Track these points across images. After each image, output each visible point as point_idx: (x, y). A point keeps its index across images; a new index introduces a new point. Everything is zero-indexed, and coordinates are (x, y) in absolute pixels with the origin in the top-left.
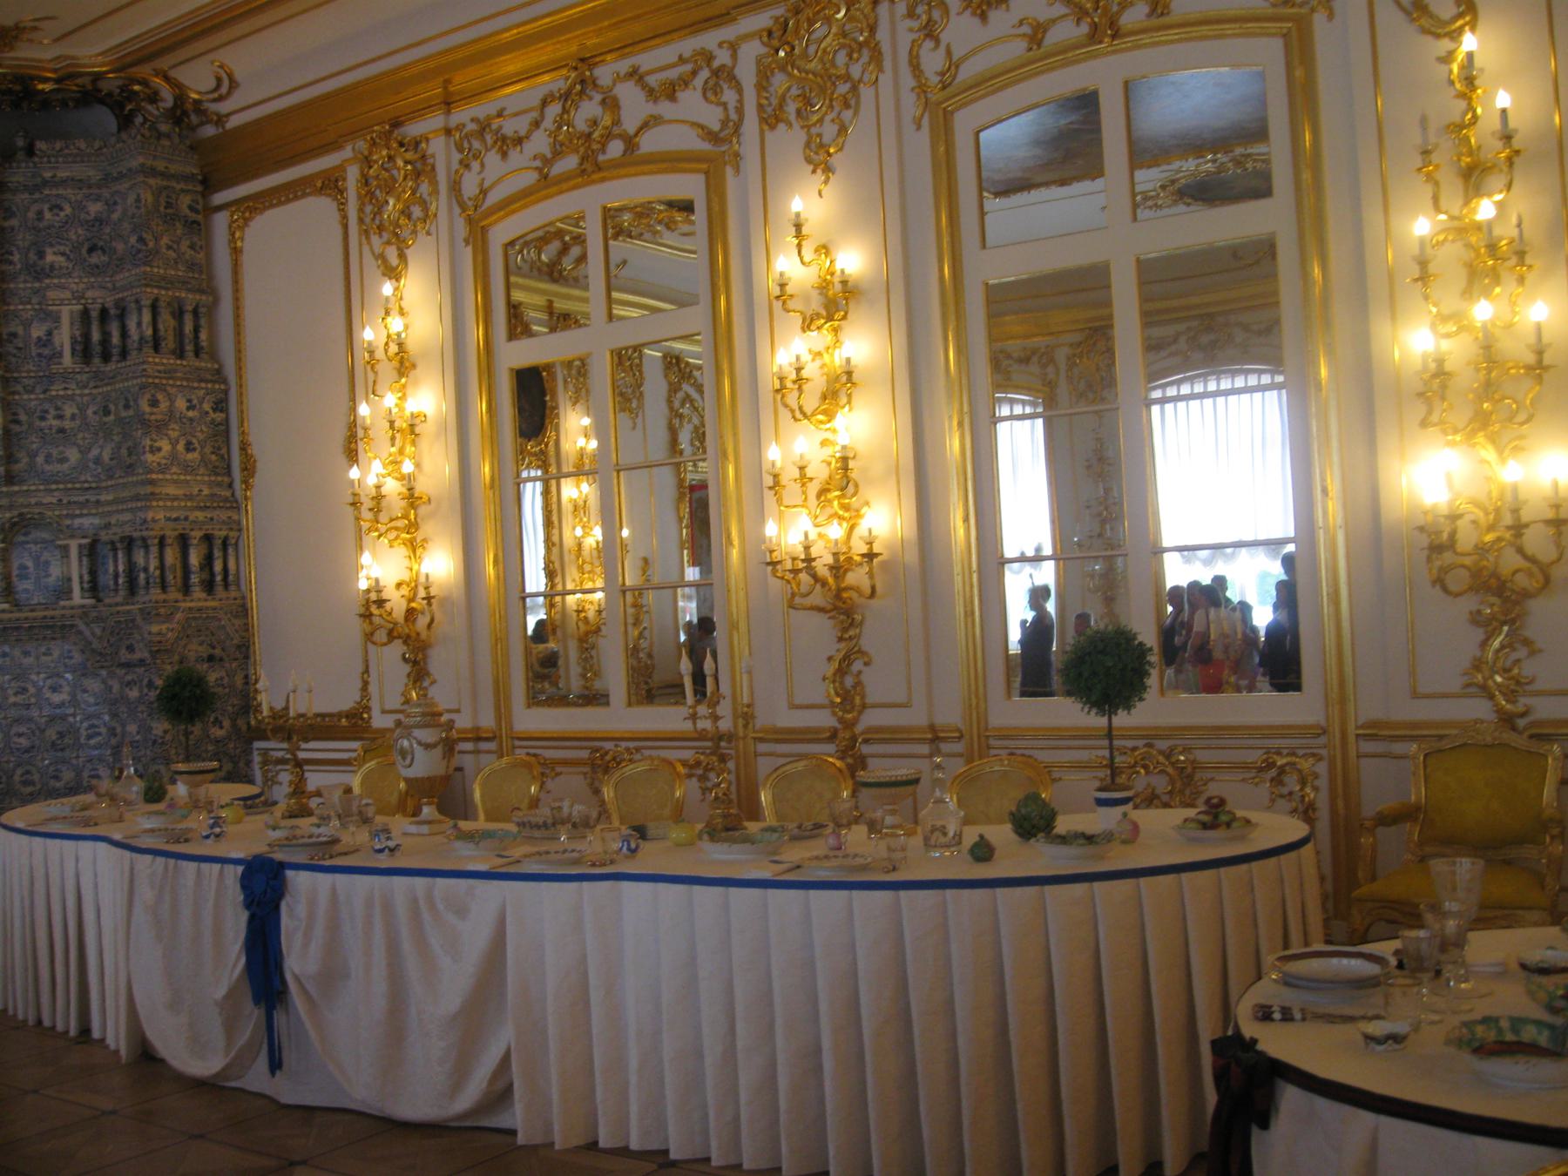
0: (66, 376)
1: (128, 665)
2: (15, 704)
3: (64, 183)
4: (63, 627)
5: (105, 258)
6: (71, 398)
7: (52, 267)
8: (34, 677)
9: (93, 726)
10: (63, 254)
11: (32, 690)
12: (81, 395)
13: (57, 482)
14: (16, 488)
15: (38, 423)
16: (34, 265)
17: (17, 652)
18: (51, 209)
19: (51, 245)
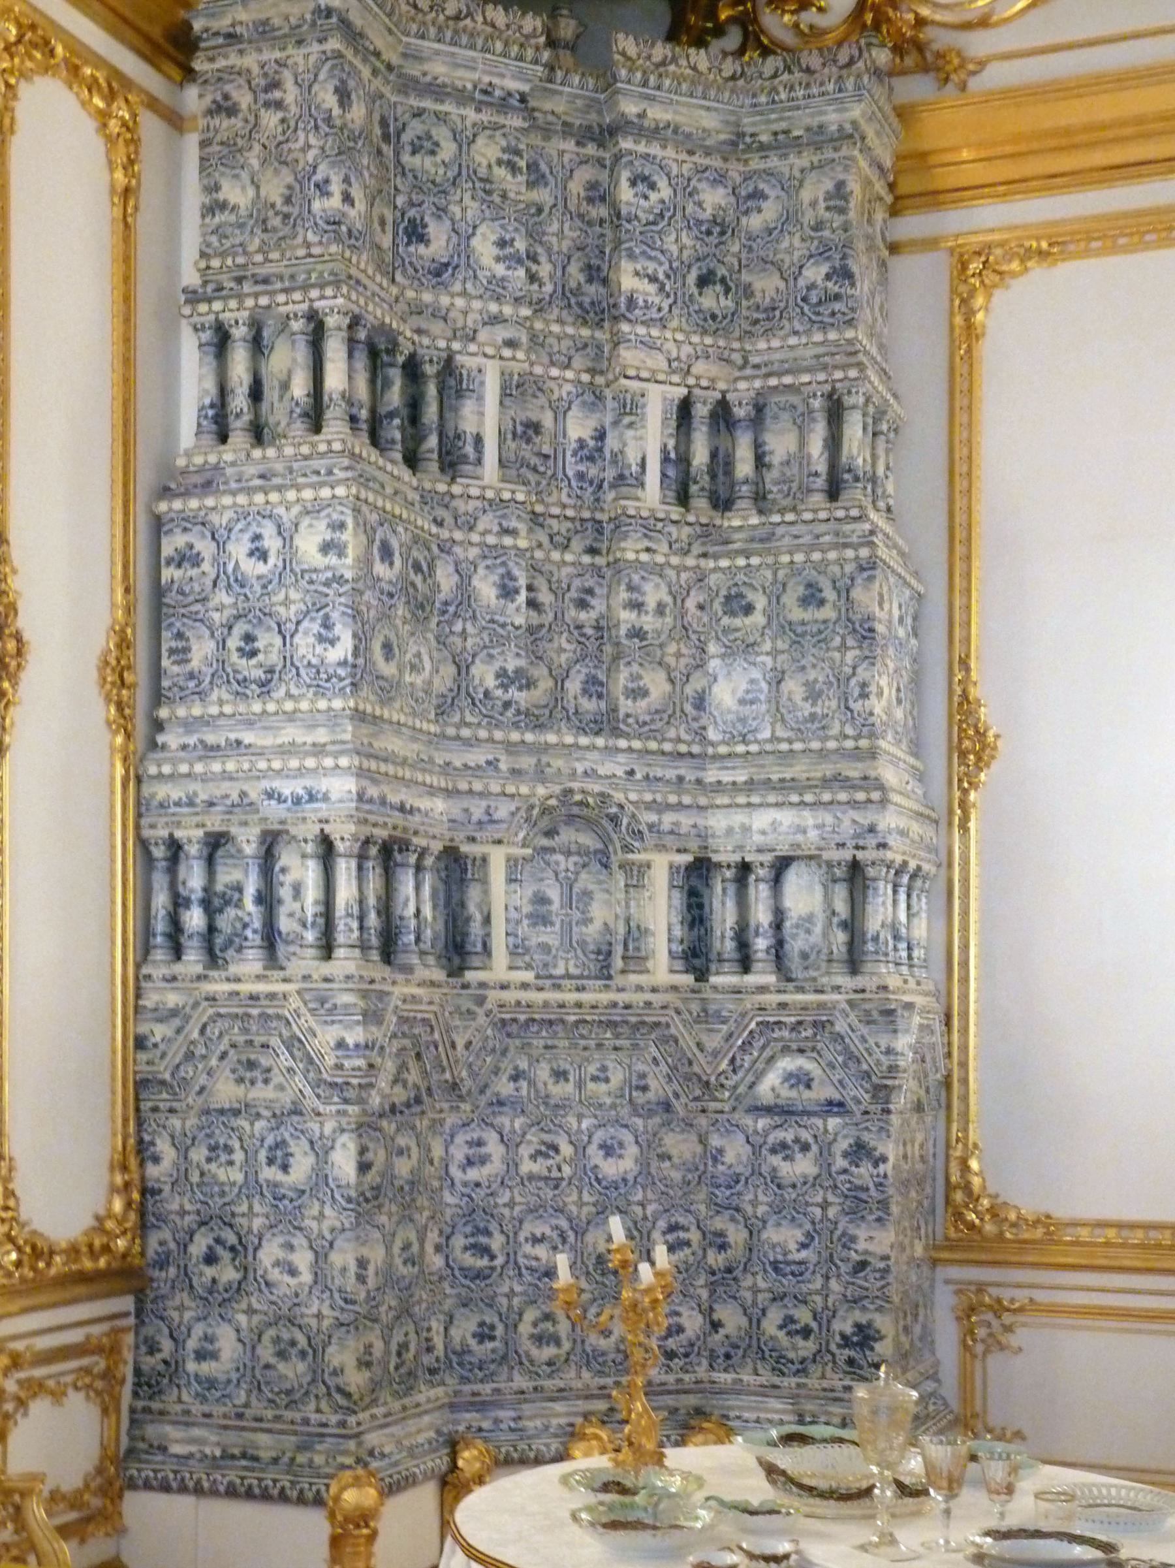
0: (650, 526)
1: (782, 1112)
2: (531, 1177)
3: (655, 133)
4: (636, 1027)
5: (727, 303)
6: (658, 570)
7: (631, 302)
8: (572, 1121)
9: (673, 1228)
10: (653, 279)
11: (566, 1150)
12: (679, 569)
13: (627, 736)
14: (552, 738)
15: (572, 613)
16: (577, 292)
17: (543, 1073)
18: (633, 183)
19: (631, 256)
